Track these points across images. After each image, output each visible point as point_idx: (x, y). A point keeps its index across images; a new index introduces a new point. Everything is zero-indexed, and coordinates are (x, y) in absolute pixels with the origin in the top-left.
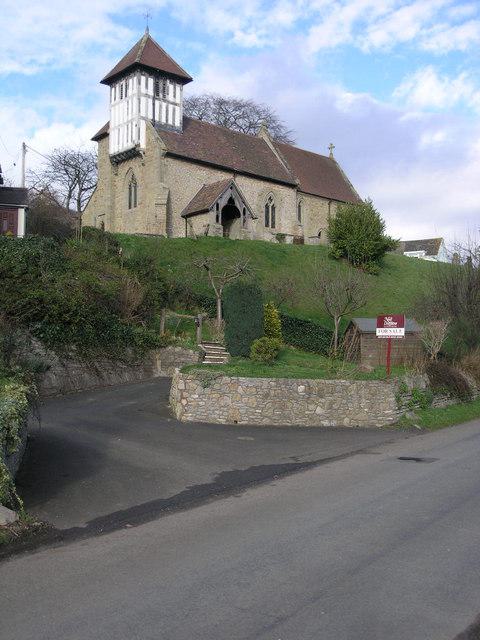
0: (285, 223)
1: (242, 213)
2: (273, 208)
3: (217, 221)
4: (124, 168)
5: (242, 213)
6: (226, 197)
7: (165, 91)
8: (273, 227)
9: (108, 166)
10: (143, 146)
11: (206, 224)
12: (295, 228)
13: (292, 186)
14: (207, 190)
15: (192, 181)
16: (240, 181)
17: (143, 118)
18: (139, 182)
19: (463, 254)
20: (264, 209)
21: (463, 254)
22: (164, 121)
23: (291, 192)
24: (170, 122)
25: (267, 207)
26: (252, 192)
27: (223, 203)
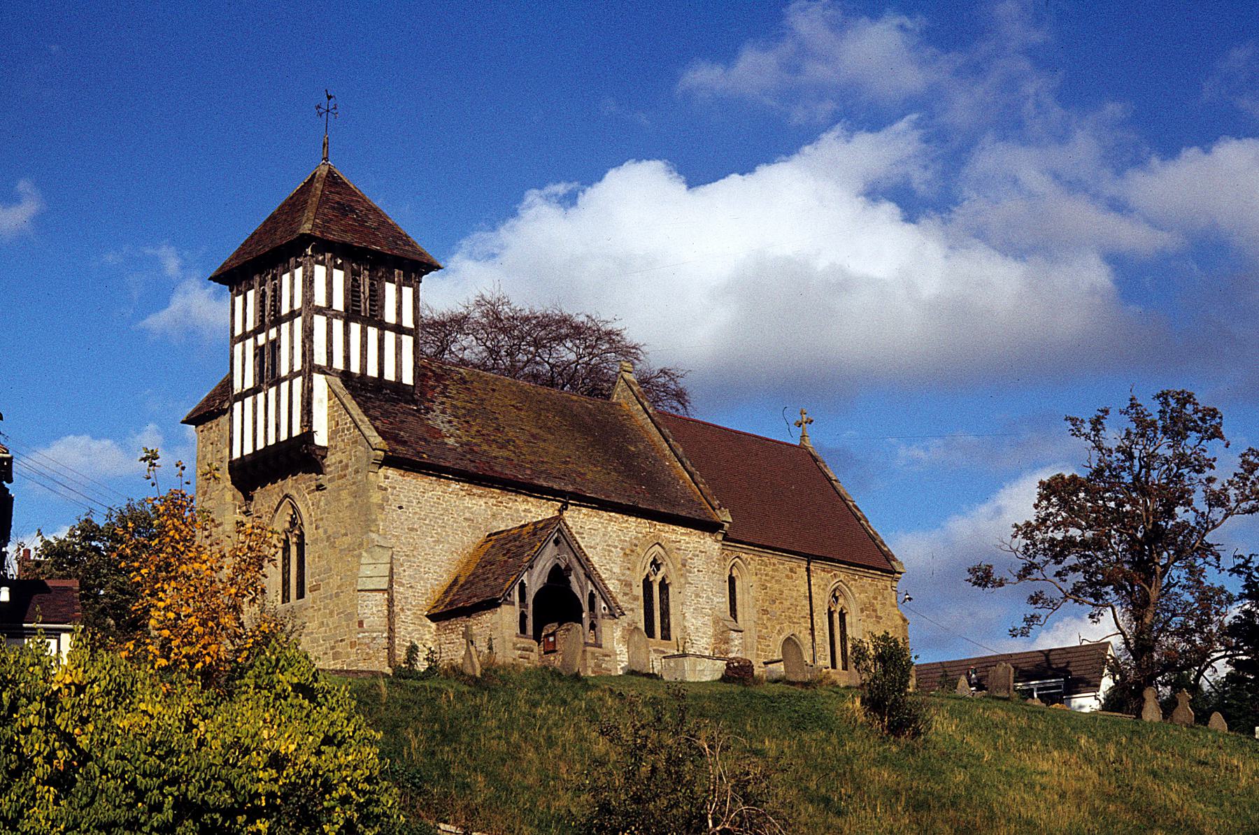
0: (695, 618)
1: (586, 607)
2: (664, 587)
3: (523, 629)
4: (267, 497)
5: (586, 607)
6: (543, 566)
7: (377, 299)
8: (666, 636)
9: (226, 491)
10: (321, 439)
11: (501, 632)
12: (722, 638)
13: (709, 527)
14: (506, 550)
15: (438, 525)
16: (581, 521)
17: (327, 370)
18: (308, 531)
19: (1083, 150)
20: (639, 591)
21: (1083, 150)
22: (372, 372)
23: (710, 544)
24: (390, 375)
25: (647, 585)
26: (607, 542)
27: (535, 580)
